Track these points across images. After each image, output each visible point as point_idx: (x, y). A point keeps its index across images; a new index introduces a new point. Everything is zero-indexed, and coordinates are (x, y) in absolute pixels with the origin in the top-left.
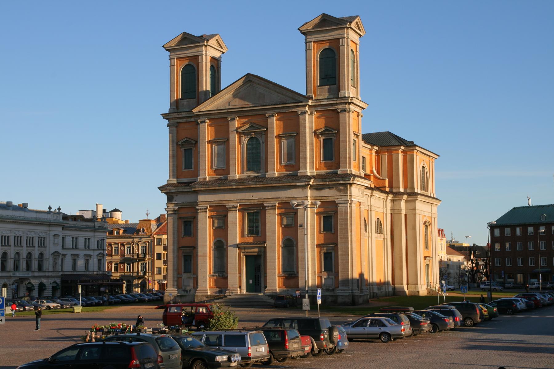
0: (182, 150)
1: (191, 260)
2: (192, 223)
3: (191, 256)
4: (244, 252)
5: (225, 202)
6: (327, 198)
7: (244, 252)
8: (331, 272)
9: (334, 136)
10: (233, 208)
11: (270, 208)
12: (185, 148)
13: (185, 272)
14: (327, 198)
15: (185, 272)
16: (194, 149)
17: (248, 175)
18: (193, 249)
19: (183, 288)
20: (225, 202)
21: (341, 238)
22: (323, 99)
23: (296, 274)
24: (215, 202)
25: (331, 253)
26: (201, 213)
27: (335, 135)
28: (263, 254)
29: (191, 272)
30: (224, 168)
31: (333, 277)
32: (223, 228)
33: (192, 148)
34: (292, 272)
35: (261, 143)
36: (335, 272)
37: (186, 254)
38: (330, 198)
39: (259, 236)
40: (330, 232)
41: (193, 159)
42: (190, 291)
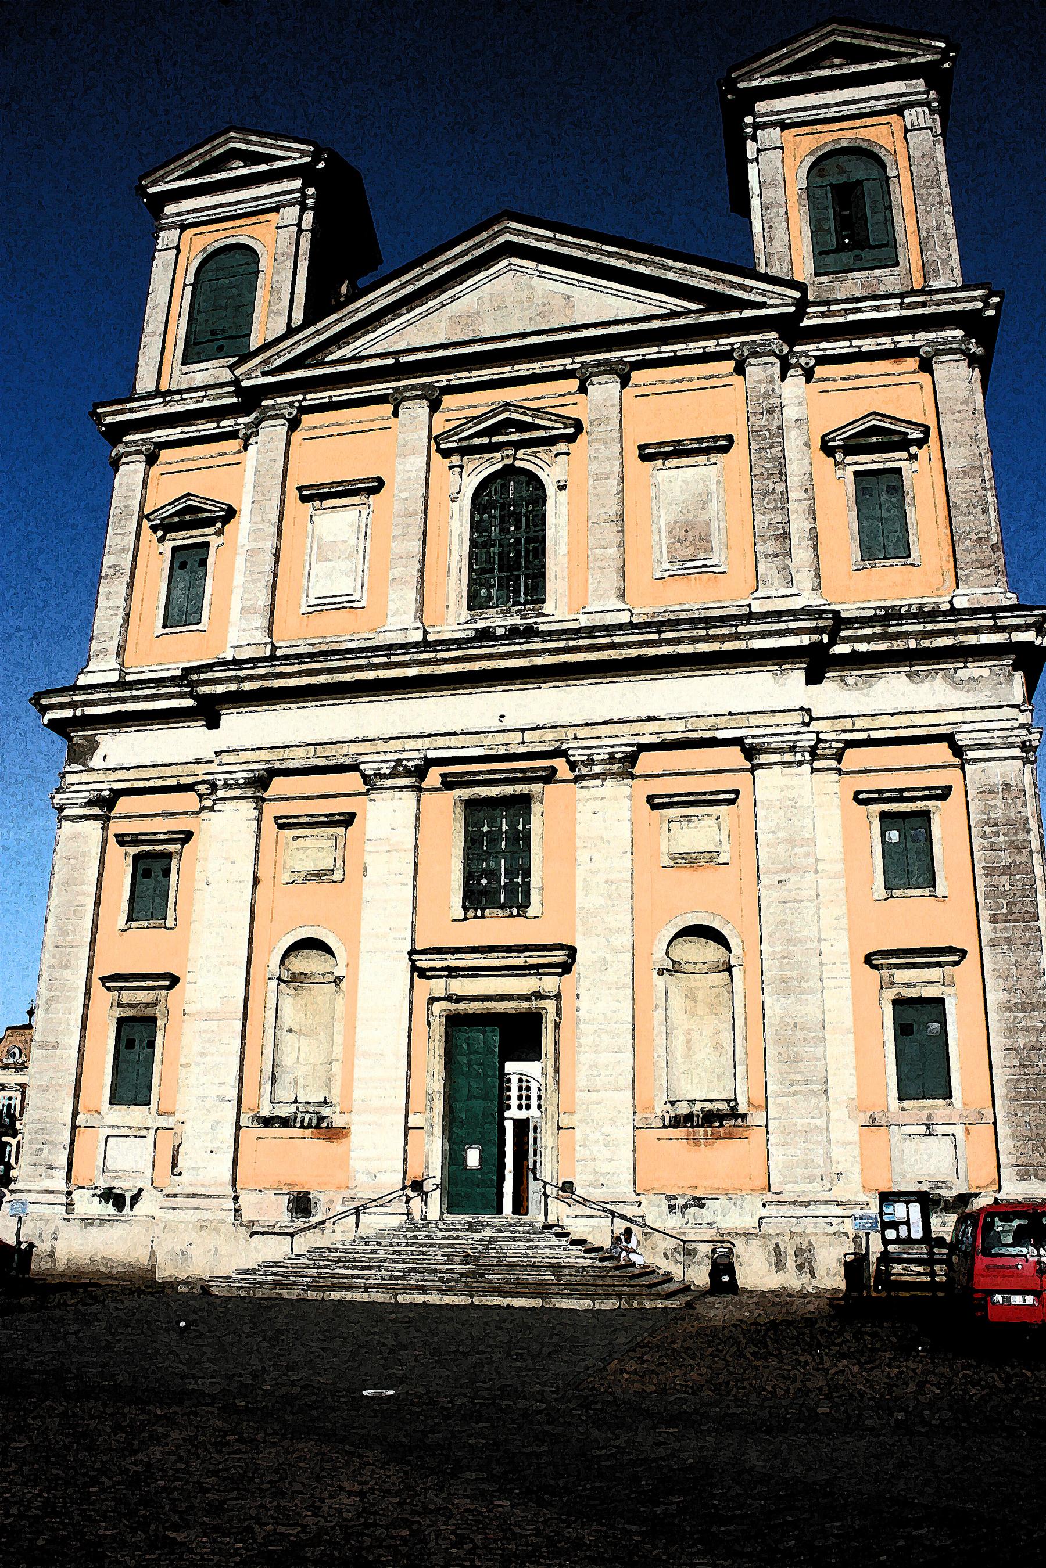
0: (161, 548)
1: (152, 1045)
2: (174, 862)
3: (153, 1020)
4: (448, 998)
5: (354, 748)
6: (904, 720)
7: (448, 998)
8: (941, 1102)
9: (913, 457)
10: (391, 776)
11: (597, 769)
12: (178, 543)
13: (115, 1099)
14: (904, 720)
15: (115, 1099)
16: (220, 540)
17: (480, 625)
18: (169, 988)
19: (103, 1183)
20: (354, 748)
21: (993, 919)
22: (858, 300)
23: (744, 1116)
24: (301, 752)
25: (940, 1001)
26: (230, 805)
27: (913, 449)
28: (550, 1005)
29: (149, 1104)
30: (355, 605)
31: (959, 1130)
32: (337, 876)
33: (208, 539)
34: (723, 1106)
35: (550, 490)
36: (965, 1104)
37: (130, 1013)
38: (918, 719)
39: (531, 912)
40: (926, 891)
41: (209, 581)
42: (135, 1199)
